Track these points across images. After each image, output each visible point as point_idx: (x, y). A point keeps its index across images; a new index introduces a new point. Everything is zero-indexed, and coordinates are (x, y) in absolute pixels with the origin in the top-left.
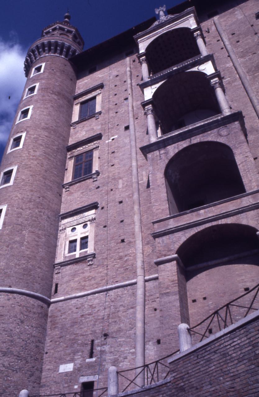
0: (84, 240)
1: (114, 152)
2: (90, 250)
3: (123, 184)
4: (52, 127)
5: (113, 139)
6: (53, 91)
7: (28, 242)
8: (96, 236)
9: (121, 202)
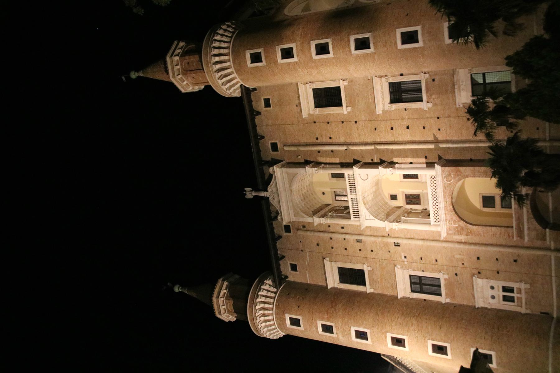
0: (505, 289)
1: (421, 259)
2: (515, 285)
3: (460, 254)
4: (380, 310)
5: (405, 257)
6: (331, 307)
7: (508, 331)
8: (505, 280)
9: (478, 258)
